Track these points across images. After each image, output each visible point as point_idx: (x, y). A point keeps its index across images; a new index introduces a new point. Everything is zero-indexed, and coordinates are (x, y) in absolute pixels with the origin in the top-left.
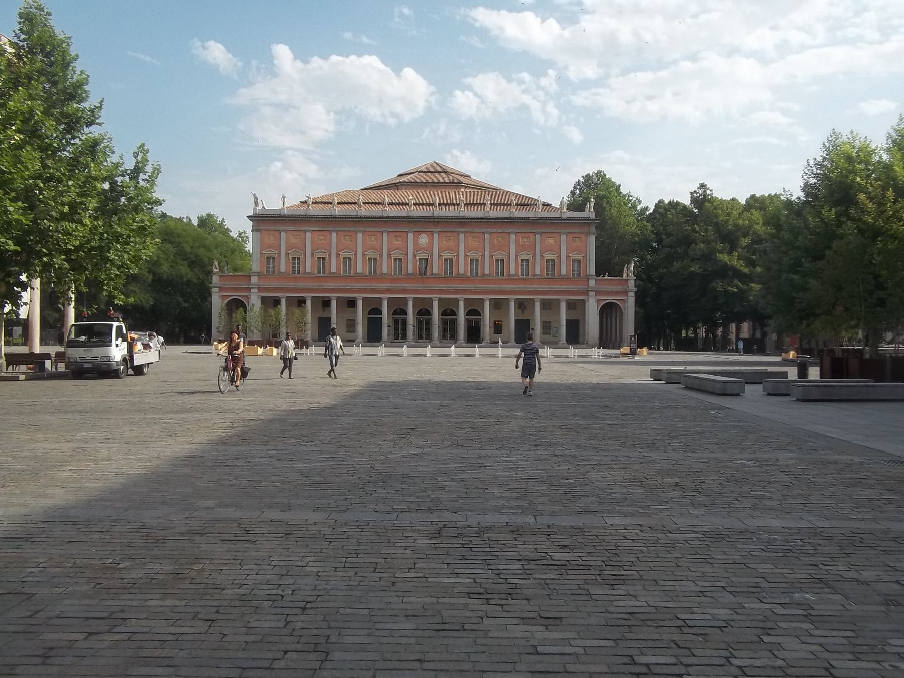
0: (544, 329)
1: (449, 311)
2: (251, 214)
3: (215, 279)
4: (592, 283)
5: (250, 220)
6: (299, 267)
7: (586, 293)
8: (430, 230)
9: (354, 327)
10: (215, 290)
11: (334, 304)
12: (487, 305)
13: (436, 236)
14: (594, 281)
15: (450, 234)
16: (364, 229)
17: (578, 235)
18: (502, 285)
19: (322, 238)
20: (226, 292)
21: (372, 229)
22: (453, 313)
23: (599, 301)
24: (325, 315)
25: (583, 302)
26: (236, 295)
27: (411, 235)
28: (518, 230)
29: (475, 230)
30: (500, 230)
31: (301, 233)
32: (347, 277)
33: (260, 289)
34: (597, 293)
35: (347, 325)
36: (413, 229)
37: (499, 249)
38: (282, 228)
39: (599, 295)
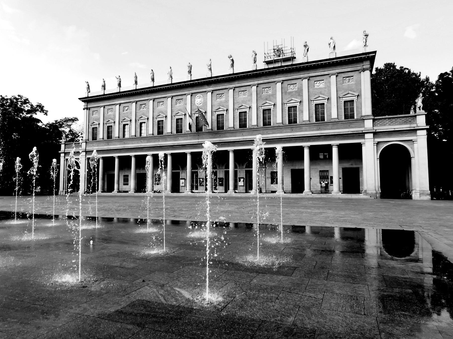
0: (320, 178)
4: (369, 124)
5: (83, 101)
7: (361, 135)
10: (62, 155)
18: (269, 134)
19: (126, 109)
27: (189, 97)
29: (243, 84)
31: (113, 107)
34: (376, 134)
37: (267, 99)
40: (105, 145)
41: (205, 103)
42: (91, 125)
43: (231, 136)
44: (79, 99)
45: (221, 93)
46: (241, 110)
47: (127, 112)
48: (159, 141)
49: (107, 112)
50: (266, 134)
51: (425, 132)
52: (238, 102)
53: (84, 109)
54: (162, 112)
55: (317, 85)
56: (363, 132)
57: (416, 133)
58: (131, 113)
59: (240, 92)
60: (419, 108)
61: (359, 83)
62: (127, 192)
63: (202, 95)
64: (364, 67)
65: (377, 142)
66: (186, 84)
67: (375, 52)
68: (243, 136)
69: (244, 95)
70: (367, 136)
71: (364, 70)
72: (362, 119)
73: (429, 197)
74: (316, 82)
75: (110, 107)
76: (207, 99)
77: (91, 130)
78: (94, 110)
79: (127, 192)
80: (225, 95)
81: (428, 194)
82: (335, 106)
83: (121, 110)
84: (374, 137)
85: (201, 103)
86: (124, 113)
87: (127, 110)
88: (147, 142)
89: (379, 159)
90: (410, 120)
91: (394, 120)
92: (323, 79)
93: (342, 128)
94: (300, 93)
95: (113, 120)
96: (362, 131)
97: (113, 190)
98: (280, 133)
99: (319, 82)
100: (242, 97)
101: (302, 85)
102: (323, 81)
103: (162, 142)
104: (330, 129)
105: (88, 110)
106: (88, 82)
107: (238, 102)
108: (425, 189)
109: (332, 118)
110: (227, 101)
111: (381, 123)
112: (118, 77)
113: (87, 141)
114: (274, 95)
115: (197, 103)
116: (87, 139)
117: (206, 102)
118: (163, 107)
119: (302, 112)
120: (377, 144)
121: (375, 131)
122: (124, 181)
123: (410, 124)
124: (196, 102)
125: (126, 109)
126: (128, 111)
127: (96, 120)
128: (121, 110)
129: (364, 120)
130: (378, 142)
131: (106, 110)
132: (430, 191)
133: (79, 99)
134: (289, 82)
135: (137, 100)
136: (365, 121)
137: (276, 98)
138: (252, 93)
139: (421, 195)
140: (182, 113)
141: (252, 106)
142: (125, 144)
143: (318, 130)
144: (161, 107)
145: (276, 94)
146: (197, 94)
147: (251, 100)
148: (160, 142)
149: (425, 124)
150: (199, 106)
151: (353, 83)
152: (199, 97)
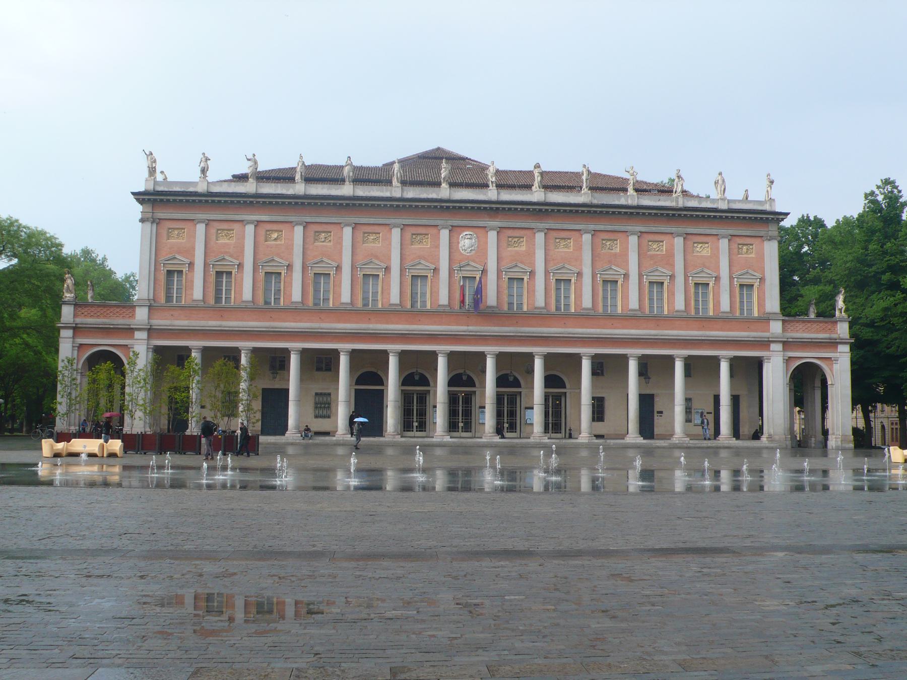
1: (417, 378)
2: (142, 189)
3: (67, 313)
4: (776, 327)
5: (138, 200)
6: (228, 291)
7: (765, 344)
8: (481, 224)
9: (329, 408)
10: (66, 334)
11: (294, 362)
12: (586, 366)
13: (492, 236)
14: (780, 324)
15: (517, 233)
16: (357, 220)
17: (748, 241)
18: (615, 328)
19: (275, 235)
20: (87, 337)
21: (372, 221)
22: (517, 384)
23: (788, 360)
24: (277, 385)
25: (758, 365)
26: (104, 343)
27: (445, 234)
28: (643, 229)
30: (609, 228)
31: (236, 226)
32: (322, 311)
33: (152, 331)
34: (787, 345)
35: (316, 403)
36: (450, 223)
39: (792, 350)
40: (211, 319)
41: (481, 251)
42: (164, 264)
43: (540, 326)
44: (133, 194)
45: (518, 235)
46: (560, 275)
47: (277, 245)
48: (369, 321)
49: (214, 237)
50: (611, 328)
51: (847, 348)
52: (553, 260)
53: (142, 220)
54: (377, 258)
55: (698, 249)
56: (770, 339)
57: (837, 348)
58: (290, 248)
59: (557, 240)
60: (840, 310)
61: (761, 257)
62: (327, 434)
63: (476, 234)
64: (770, 233)
65: (787, 358)
66: (443, 205)
67: (788, 214)
68: (566, 327)
69: (567, 246)
70: (773, 347)
71: (771, 239)
72: (765, 319)
73: (852, 445)
74: (695, 245)
75: (225, 226)
76: (486, 243)
77: (162, 277)
78: (171, 227)
79: (327, 434)
80: (526, 241)
81: (850, 441)
82: (726, 290)
83: (261, 238)
84: (784, 350)
85: (473, 248)
86: (268, 246)
88: (339, 322)
89: (788, 386)
90: (829, 327)
91: (809, 325)
92: (708, 241)
93: (738, 330)
94: (669, 259)
95: (237, 259)
96: (769, 338)
97: (285, 428)
98: (636, 329)
99: (701, 245)
100: (563, 249)
101: (673, 245)
102: (707, 245)
103: (377, 323)
104: (718, 330)
105: (155, 226)
106: (151, 154)
107: (553, 260)
108: (847, 434)
109: (722, 310)
110: (531, 254)
111: (792, 328)
112: (250, 156)
113: (152, 302)
114: (624, 256)
115: (463, 248)
116: (151, 297)
117: (486, 249)
118: (378, 245)
119: (673, 294)
120: (787, 360)
121: (786, 340)
122: (316, 408)
123: (830, 334)
124: (460, 245)
125: (275, 235)
126: (279, 242)
127: (179, 253)
128: (261, 238)
129: (770, 319)
130: (790, 357)
131: (213, 231)
132: (853, 436)
133: (133, 194)
134: (651, 237)
135: (308, 219)
136: (771, 321)
137: (627, 262)
138: (582, 245)
139: (843, 442)
140: (427, 264)
141: (582, 270)
142: (272, 319)
143: (699, 329)
144: (373, 245)
145: (627, 255)
146: (463, 229)
147: (579, 259)
148: (371, 323)
149: (848, 336)
150: (468, 254)
151: (753, 255)
152: (468, 236)
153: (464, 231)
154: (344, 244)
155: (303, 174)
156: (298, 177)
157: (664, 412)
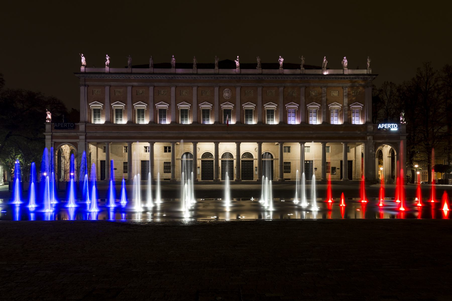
27: (217, 89)
38: (106, 83)
67: (377, 75)
87: (142, 93)
105: (86, 88)
124: (224, 95)
153: (225, 89)
154: (172, 95)
155: (152, 64)
156: (150, 65)
157: (317, 169)
